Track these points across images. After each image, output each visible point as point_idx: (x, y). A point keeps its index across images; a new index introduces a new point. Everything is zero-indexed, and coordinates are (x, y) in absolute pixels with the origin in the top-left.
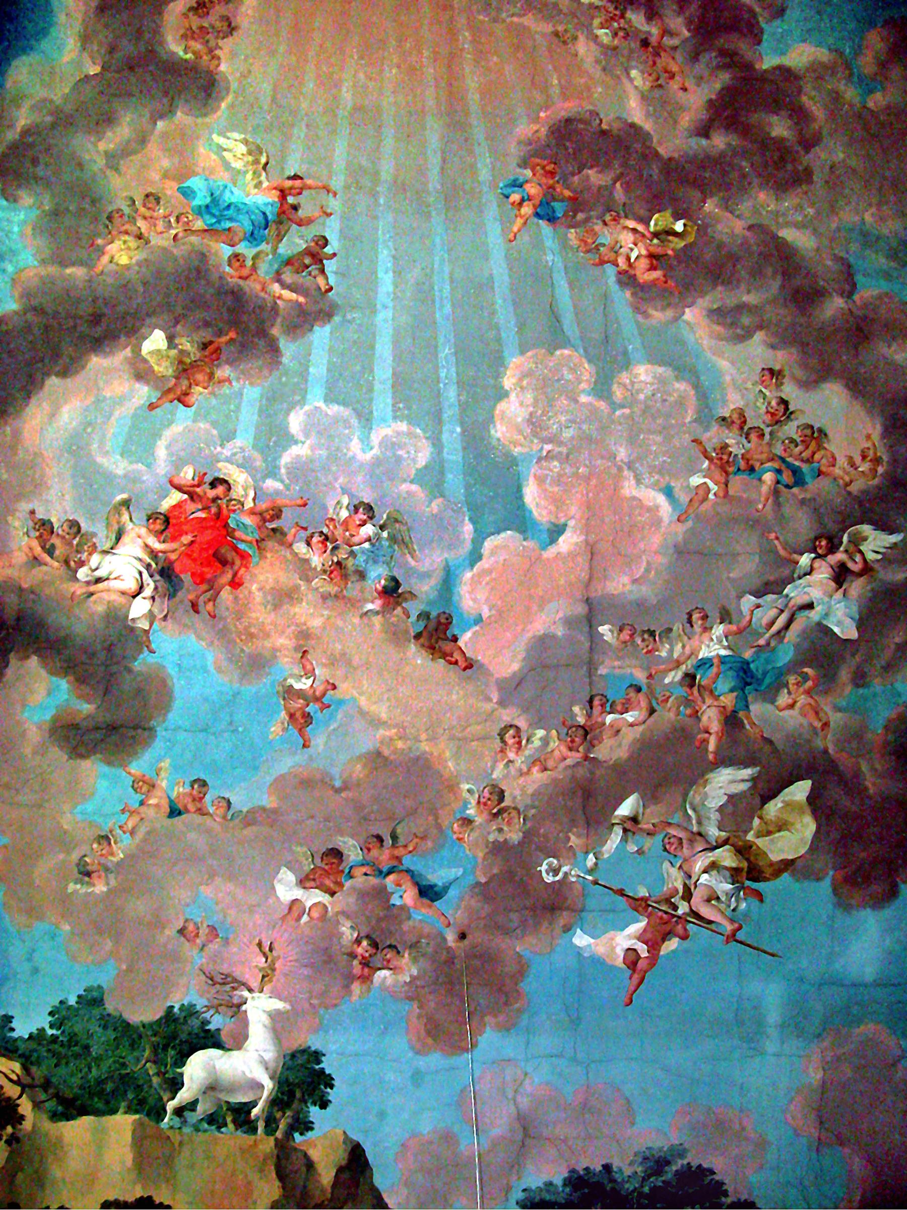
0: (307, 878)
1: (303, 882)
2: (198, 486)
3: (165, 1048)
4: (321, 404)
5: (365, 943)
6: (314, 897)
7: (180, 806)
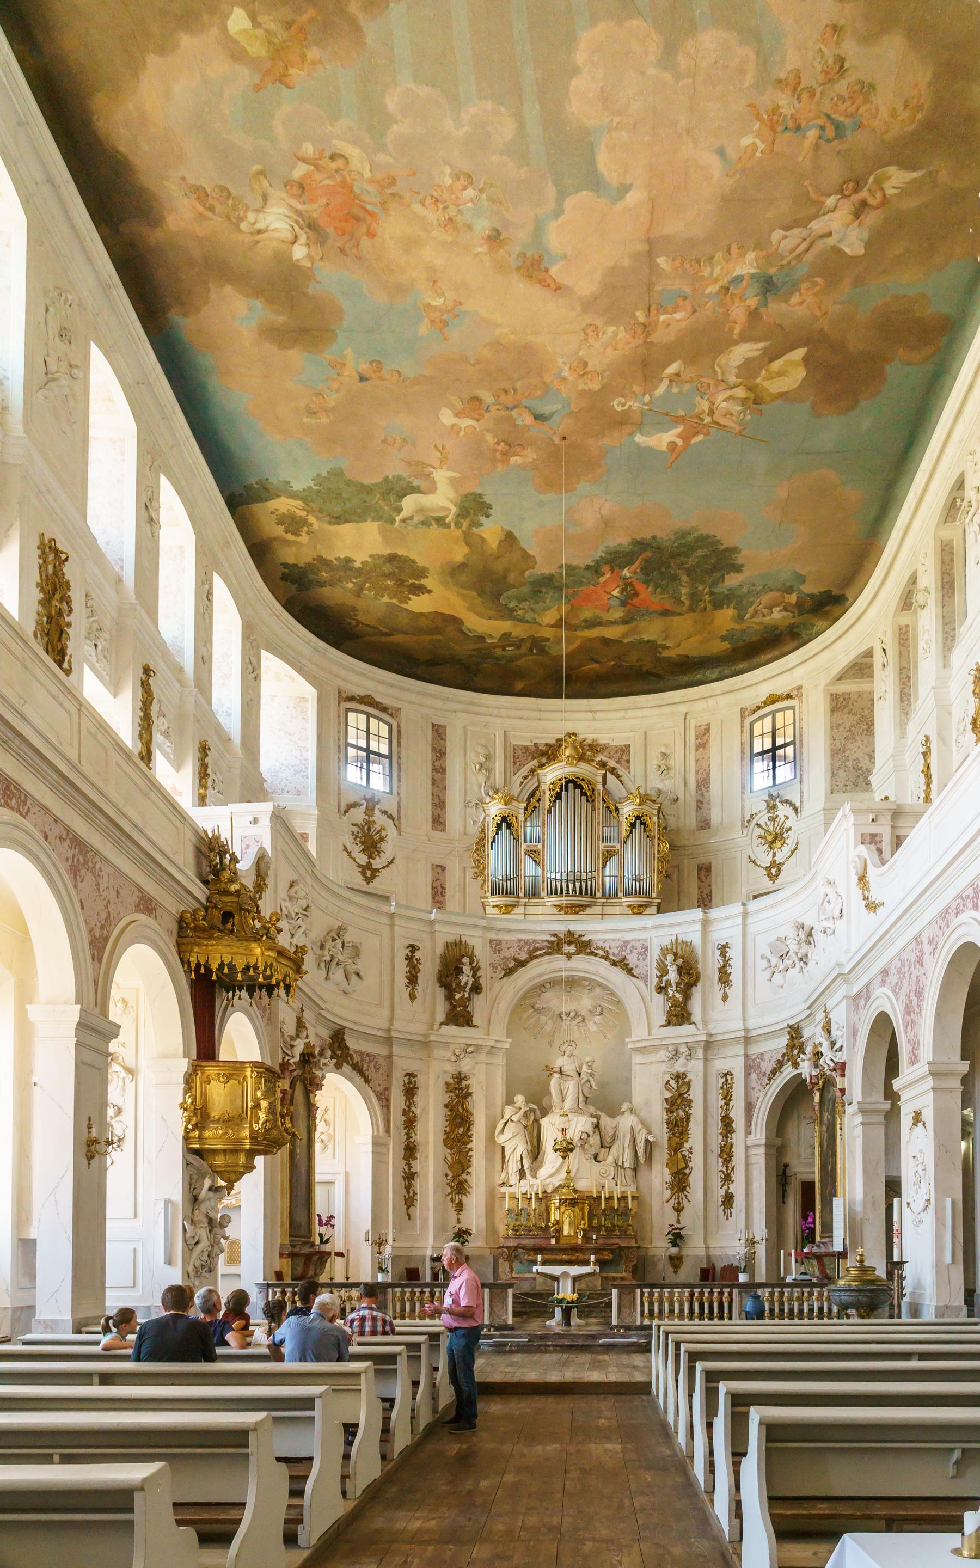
0: (460, 412)
1: (457, 415)
2: (320, 159)
3: (388, 494)
4: (411, 85)
5: (502, 444)
6: (466, 423)
7: (367, 375)
